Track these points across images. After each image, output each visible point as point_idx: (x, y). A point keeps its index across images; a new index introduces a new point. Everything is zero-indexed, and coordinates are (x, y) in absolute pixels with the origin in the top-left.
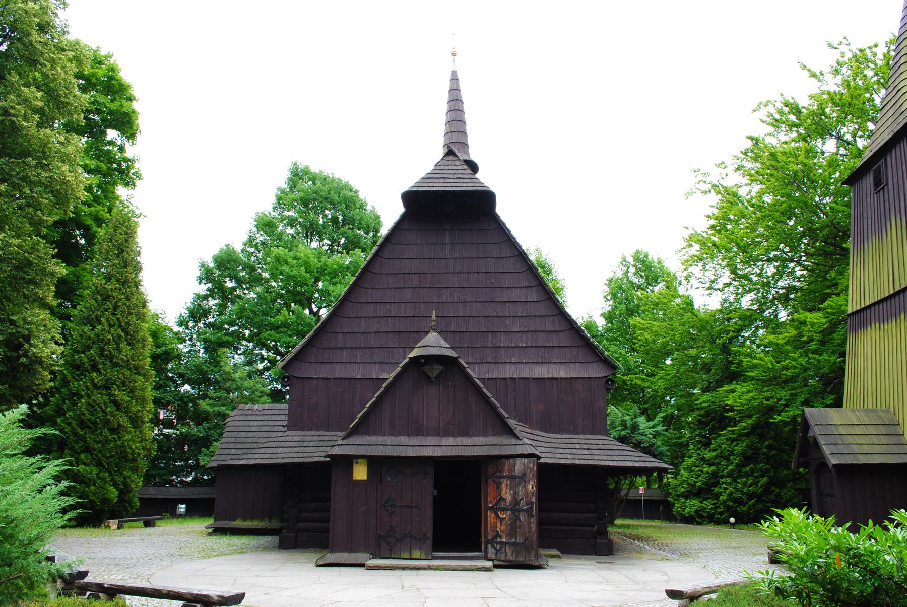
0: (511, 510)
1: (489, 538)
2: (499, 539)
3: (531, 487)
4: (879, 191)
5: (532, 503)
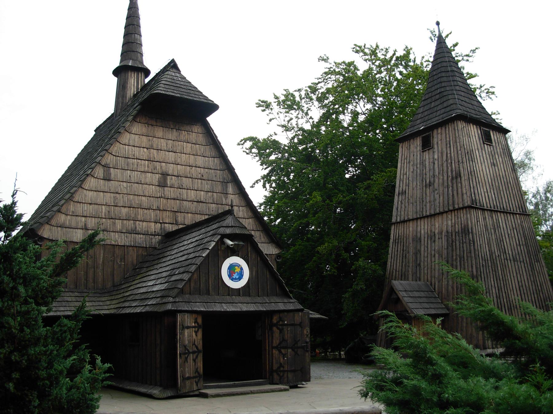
4: (425, 151)
5: (307, 343)
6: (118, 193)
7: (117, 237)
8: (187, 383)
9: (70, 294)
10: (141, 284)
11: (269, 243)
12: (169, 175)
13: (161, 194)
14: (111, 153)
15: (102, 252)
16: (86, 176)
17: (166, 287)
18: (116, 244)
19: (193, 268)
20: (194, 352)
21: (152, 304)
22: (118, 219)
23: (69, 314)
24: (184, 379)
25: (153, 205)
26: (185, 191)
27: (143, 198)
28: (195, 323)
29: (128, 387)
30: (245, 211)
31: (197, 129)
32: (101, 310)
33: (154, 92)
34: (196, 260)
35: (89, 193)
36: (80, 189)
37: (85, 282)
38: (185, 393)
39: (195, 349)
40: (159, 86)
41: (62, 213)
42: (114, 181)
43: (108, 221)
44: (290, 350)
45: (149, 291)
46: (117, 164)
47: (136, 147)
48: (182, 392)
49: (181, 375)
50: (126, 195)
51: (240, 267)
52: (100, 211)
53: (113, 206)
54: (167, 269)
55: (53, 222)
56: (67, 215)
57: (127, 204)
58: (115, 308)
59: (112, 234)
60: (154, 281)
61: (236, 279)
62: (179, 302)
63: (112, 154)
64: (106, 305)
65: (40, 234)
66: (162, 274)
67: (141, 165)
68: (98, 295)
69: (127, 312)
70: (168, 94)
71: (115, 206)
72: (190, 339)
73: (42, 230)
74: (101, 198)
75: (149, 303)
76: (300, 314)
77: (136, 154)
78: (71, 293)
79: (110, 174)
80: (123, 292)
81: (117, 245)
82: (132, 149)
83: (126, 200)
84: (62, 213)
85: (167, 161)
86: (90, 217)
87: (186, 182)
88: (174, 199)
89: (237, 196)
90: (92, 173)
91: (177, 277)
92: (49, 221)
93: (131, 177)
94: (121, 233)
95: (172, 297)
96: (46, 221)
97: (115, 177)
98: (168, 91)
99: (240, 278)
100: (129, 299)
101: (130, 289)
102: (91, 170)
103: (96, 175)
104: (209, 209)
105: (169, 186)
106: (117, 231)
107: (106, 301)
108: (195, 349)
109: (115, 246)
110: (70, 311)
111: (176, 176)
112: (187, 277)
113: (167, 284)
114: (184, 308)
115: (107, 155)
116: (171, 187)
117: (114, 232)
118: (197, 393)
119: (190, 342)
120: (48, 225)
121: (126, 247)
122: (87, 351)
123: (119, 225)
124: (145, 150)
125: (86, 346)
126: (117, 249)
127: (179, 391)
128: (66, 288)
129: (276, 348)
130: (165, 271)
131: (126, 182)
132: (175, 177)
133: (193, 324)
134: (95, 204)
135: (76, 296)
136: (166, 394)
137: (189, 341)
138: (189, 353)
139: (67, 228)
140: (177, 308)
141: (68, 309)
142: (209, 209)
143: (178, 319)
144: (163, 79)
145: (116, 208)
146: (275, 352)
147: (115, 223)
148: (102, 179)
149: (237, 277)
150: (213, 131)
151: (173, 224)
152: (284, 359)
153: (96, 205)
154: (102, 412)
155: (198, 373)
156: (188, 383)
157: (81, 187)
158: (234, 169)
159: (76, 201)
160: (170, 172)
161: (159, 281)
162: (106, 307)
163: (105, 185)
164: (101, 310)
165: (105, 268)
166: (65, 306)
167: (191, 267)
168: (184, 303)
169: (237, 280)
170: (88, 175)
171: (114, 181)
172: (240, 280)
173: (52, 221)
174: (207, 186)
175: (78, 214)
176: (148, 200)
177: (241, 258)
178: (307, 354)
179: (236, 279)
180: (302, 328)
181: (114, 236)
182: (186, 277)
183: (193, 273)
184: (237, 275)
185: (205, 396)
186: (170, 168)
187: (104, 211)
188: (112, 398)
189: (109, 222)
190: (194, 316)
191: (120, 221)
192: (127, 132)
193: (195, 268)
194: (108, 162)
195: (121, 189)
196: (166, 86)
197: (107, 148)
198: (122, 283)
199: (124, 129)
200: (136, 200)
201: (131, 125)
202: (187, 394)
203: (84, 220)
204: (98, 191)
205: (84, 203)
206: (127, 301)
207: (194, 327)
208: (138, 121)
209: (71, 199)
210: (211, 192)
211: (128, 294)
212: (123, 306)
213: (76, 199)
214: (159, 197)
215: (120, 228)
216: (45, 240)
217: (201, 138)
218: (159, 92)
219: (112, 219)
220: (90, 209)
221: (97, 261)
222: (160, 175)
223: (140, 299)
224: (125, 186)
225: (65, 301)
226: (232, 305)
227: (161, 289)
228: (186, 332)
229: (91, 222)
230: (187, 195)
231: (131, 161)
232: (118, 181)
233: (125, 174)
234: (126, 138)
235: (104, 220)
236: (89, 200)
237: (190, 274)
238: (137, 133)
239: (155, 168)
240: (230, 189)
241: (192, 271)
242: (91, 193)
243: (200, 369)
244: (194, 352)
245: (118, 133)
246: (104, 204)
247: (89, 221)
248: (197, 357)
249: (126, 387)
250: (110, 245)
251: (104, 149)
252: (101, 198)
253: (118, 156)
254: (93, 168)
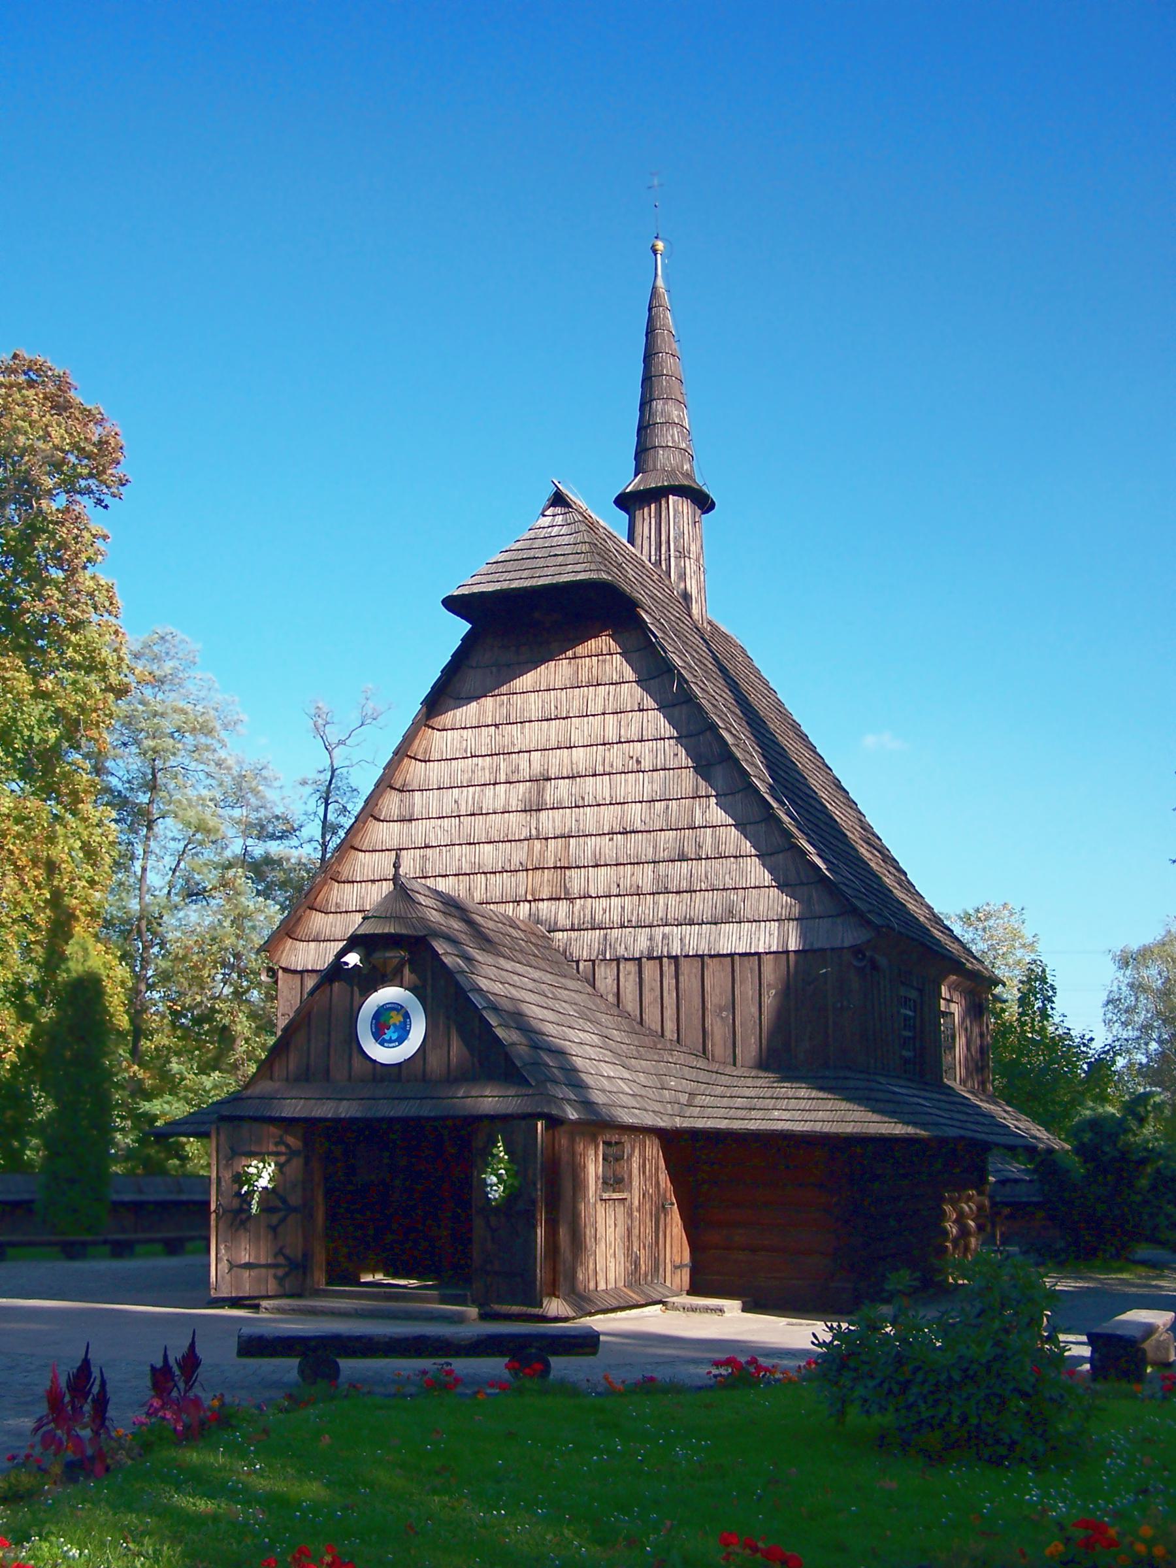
11: (838, 915)
51: (403, 1011)
61: (391, 1041)
89: (739, 796)
99: (401, 1040)
104: (655, 847)
149: (395, 1036)
151: (559, 899)
172: (399, 1044)
174: (648, 785)
205: (360, 882)
210: (661, 800)
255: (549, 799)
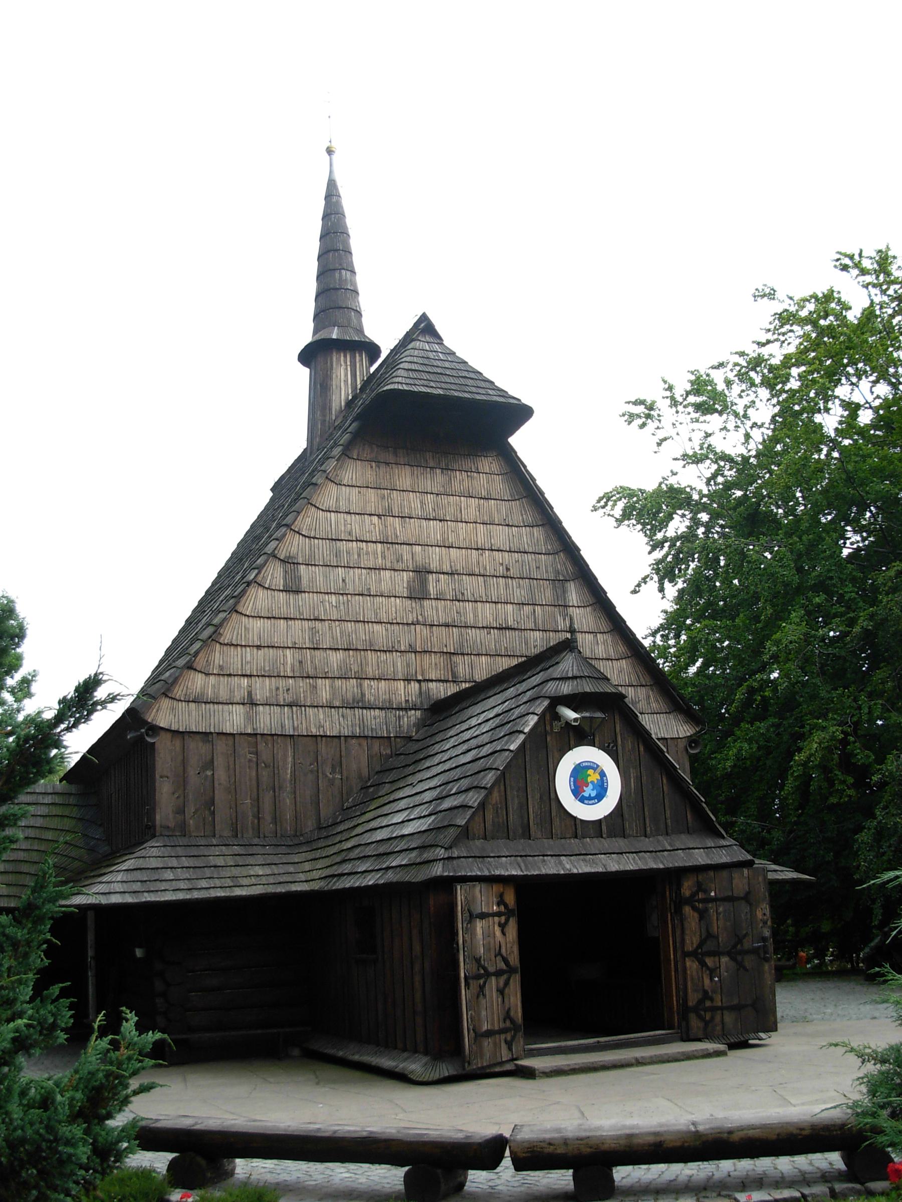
0: (729, 954)
1: (690, 1004)
2: (708, 1004)
3: (763, 911)
5: (764, 939)
6: (318, 620)
7: (322, 717)
8: (486, 1044)
9: (222, 851)
10: (379, 820)
12: (432, 573)
13: (415, 615)
14: (298, 533)
15: (290, 753)
16: (245, 585)
17: (430, 825)
18: (322, 733)
19: (489, 778)
20: (498, 973)
21: (400, 866)
22: (322, 678)
23: (219, 895)
24: (479, 1036)
25: (399, 642)
26: (469, 606)
27: (377, 627)
28: (498, 905)
29: (356, 1058)
30: (609, 641)
31: (489, 464)
32: (291, 882)
33: (385, 388)
34: (495, 761)
35: (255, 622)
36: (234, 615)
37: (256, 821)
38: (483, 1068)
39: (502, 966)
40: (394, 374)
41: (195, 670)
42: (309, 592)
43: (301, 683)
44: (725, 960)
45: (394, 835)
46: (312, 554)
47: (353, 515)
48: (475, 1067)
49: (471, 1027)
50: (337, 623)
51: (599, 770)
52: (282, 662)
53: (309, 648)
54: (433, 783)
55: (178, 692)
56: (207, 674)
57: (340, 643)
58: (322, 878)
59: (310, 711)
60: (406, 813)
61: (590, 798)
62: (459, 858)
63: (300, 534)
64: (302, 872)
65: (149, 720)
66: (423, 795)
67: (367, 553)
68: (283, 850)
69: (347, 886)
70: (416, 390)
71: (314, 649)
72: (489, 943)
73: (155, 710)
74: (281, 632)
75: (394, 864)
76: (745, 871)
77: (354, 531)
78: (224, 848)
79: (300, 578)
80: (340, 842)
81: (322, 736)
82: (345, 521)
83: (339, 635)
84: (195, 670)
85: (424, 540)
86: (258, 676)
87: (471, 586)
88: (447, 625)
90: (259, 579)
91: (455, 800)
92: (168, 689)
93: (347, 581)
94: (331, 707)
95: (442, 847)
96: (163, 691)
97: (311, 585)
98: (415, 385)
99: (600, 797)
100: (353, 855)
101: (354, 833)
102: (256, 571)
103: (268, 582)
104: (526, 644)
105: (432, 597)
106: (321, 704)
107: (301, 862)
108: (502, 966)
109: (319, 738)
110: (221, 887)
111: (447, 573)
112: (475, 801)
113: (433, 817)
114: (471, 872)
115: (289, 536)
116: (437, 599)
117: (315, 707)
118: (509, 1067)
119: (489, 949)
120: (167, 700)
121: (342, 738)
122: (65, 1002)
123: (325, 690)
124: (375, 519)
125: (62, 990)
126: (322, 746)
127: (466, 1065)
128: (214, 836)
129: (694, 954)
130: (430, 789)
131: (335, 593)
132: (446, 576)
133: (495, 908)
134: (268, 647)
135: (236, 855)
136: (438, 1070)
137: (487, 948)
138: (488, 974)
139: (209, 703)
140: (455, 871)
141: (218, 883)
142: (526, 644)
143: (459, 898)
144: (403, 360)
145: (317, 653)
146: (692, 965)
147: (316, 688)
148: (282, 591)
149: (593, 794)
150: (525, 467)
151: (447, 681)
152: (711, 979)
153: (271, 650)
154: (270, 1124)
155: (512, 1021)
156: (487, 1044)
157: (237, 612)
158: (578, 550)
159: (226, 642)
160: (434, 566)
161: (416, 813)
162: (302, 877)
163: (288, 604)
164: (291, 882)
165: (298, 787)
166: (210, 878)
167: (484, 777)
168: (470, 859)
169: (593, 801)
170: (249, 584)
171: (309, 592)
172: (599, 801)
173: (175, 691)
174: (519, 592)
175: (232, 672)
176: (387, 630)
177: (599, 748)
178: (766, 967)
179: (590, 798)
180: (750, 904)
181: (315, 714)
182: (473, 799)
183: (490, 790)
184: (593, 790)
185: (528, 1074)
186: (434, 556)
187: (289, 662)
188: (318, 1084)
189: (301, 685)
190: (496, 888)
191: (327, 680)
192: (332, 481)
193: (494, 778)
194: (294, 550)
195: (325, 610)
196: (411, 374)
197: (288, 520)
198: (338, 820)
199: (325, 475)
200: (360, 634)
201: (341, 467)
202: (488, 1071)
203: (246, 684)
204: (274, 618)
206: (347, 860)
207: (499, 914)
208: (355, 457)
209: (214, 638)
210: (528, 604)
211: (349, 845)
212: (339, 872)
213: (225, 639)
214: (413, 624)
215: (328, 697)
216: (162, 733)
217: (499, 485)
218: (396, 387)
219: (308, 677)
220: (258, 659)
221: (279, 773)
222: (411, 573)
223: (374, 856)
224: (334, 604)
225: (210, 867)
226: (584, 860)
227: (419, 830)
228: (479, 925)
229: (262, 688)
230: (476, 616)
231: (343, 546)
232: (317, 592)
233: (332, 578)
234: (329, 495)
235: (291, 681)
236: (255, 639)
237: (483, 793)
238: (354, 483)
239: (399, 559)
240: (574, 594)
241: (486, 784)
242: (259, 623)
243: (516, 1012)
244: (498, 973)
245: (311, 487)
246: (290, 646)
247: (258, 685)
248: (507, 983)
249: (351, 1058)
250: (308, 736)
251: (284, 523)
252: (281, 632)
253: (314, 538)
254: (260, 568)
255: (432, 590)
